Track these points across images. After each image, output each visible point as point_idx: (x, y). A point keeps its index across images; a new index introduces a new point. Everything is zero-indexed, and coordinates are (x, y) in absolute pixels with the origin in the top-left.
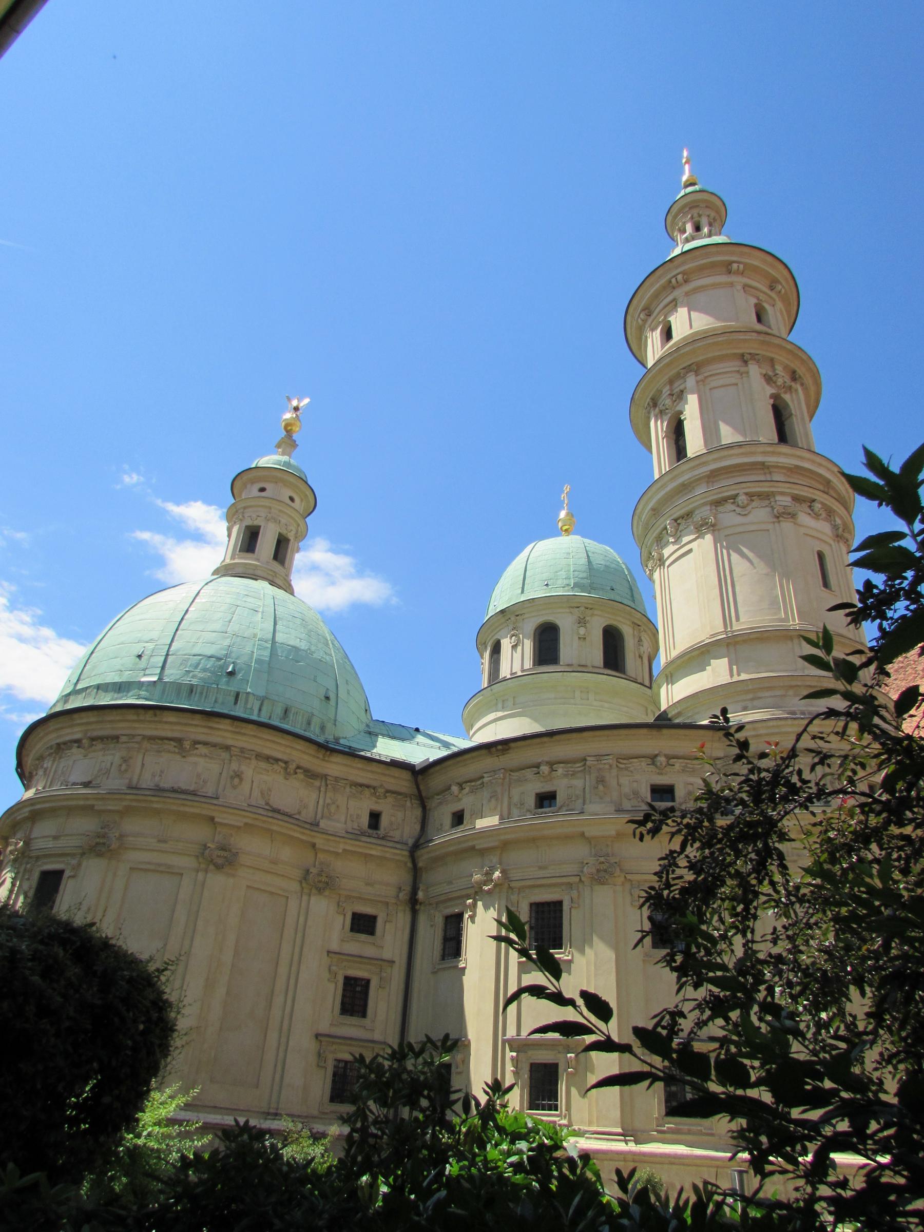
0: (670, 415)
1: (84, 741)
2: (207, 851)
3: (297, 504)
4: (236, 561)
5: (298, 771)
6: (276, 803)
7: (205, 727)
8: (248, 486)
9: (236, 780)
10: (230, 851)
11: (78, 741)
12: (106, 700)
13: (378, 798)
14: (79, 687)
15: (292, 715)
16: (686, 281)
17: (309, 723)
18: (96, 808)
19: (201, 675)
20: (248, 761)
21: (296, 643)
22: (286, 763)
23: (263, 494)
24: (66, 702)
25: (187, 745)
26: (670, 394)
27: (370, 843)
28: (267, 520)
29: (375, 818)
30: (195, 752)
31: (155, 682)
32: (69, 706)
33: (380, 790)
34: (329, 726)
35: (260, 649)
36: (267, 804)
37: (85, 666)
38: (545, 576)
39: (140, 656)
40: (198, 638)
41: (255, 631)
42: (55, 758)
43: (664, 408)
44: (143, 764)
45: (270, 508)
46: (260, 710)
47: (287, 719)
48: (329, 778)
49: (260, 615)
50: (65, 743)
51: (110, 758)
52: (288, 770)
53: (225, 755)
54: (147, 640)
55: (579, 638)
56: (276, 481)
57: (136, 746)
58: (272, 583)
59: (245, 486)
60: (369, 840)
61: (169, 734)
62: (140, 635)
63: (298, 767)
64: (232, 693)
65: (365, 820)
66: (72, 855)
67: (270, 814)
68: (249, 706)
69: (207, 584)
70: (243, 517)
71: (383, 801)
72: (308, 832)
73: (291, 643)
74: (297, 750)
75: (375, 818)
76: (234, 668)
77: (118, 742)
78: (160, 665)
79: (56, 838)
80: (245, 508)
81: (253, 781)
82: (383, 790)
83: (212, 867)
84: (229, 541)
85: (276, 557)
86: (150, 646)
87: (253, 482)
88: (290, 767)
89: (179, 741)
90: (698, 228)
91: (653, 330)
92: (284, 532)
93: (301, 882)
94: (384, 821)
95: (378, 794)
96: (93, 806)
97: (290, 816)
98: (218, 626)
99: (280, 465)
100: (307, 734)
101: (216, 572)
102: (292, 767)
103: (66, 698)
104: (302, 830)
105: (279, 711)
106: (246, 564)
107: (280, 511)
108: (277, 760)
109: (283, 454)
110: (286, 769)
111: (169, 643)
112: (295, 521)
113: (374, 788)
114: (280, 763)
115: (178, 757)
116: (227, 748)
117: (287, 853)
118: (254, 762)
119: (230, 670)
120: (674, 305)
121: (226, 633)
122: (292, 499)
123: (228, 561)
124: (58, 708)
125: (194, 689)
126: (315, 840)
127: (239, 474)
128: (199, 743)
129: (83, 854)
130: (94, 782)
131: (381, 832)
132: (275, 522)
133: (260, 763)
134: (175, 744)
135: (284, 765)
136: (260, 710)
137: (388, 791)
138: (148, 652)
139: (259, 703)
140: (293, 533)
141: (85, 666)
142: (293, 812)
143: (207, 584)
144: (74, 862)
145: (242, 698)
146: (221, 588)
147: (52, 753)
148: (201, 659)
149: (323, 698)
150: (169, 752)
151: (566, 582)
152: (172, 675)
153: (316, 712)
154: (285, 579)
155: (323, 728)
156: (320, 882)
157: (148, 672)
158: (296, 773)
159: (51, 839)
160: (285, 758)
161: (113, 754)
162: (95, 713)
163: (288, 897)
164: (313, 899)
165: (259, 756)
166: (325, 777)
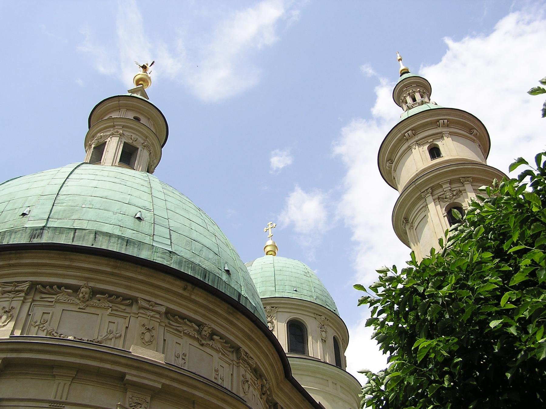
0: (448, 203)
7: (227, 320)
11: (76, 289)
16: (448, 126)
18: (128, 377)
25: (206, 332)
26: (450, 190)
30: (211, 343)
38: (294, 284)
42: (25, 299)
43: (444, 196)
44: (165, 340)
45: (147, 137)
55: (322, 339)
59: (118, 108)
77: (131, 305)
87: (129, 108)
89: (200, 325)
90: (414, 100)
91: (419, 143)
96: (124, 375)
115: (196, 344)
120: (441, 136)
150: (188, 335)
151: (310, 294)
162: (112, 262)
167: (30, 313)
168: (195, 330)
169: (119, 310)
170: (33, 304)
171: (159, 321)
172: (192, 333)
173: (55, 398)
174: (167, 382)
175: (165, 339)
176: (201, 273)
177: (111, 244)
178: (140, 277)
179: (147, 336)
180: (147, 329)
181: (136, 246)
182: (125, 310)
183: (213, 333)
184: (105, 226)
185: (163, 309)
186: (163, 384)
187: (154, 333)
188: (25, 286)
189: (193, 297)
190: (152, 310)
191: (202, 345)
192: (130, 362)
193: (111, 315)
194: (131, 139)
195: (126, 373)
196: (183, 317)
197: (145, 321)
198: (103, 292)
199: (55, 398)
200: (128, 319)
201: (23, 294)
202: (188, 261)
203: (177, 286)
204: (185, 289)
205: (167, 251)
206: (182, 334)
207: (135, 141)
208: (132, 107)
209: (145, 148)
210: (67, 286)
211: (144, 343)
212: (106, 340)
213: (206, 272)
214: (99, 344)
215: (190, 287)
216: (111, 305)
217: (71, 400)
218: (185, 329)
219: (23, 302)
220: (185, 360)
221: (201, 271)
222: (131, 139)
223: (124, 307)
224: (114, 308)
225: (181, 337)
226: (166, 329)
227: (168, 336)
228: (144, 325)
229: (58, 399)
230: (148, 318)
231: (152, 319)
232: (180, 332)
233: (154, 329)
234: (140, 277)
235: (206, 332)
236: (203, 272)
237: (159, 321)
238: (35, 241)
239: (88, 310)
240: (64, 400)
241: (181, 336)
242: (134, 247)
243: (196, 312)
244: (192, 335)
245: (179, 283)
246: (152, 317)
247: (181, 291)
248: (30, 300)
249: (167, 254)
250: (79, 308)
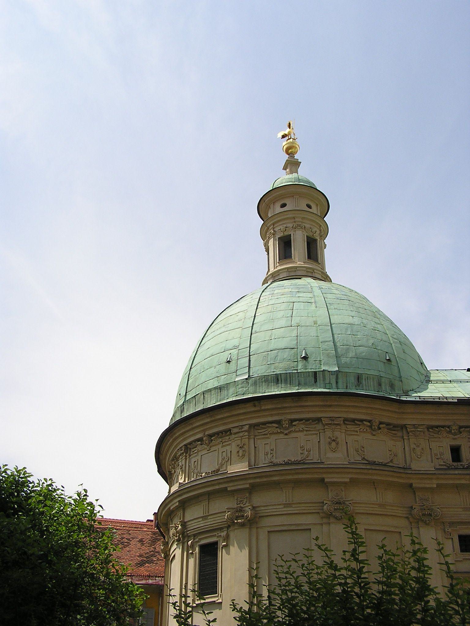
2: (325, 507)
3: (314, 210)
4: (279, 268)
5: (381, 426)
6: (371, 457)
8: (272, 206)
9: (334, 444)
10: (344, 503)
12: (212, 402)
13: (455, 434)
14: (188, 397)
15: (364, 380)
17: (380, 385)
18: (229, 489)
19: (281, 365)
20: (339, 427)
21: (349, 320)
22: (370, 421)
23: (285, 209)
24: (182, 411)
25: (286, 425)
27: (459, 474)
28: (294, 228)
29: (456, 452)
30: (293, 429)
31: (246, 379)
32: (185, 414)
33: (454, 428)
34: (397, 383)
35: (323, 333)
36: (364, 459)
37: (188, 380)
39: (229, 362)
40: (271, 336)
41: (314, 319)
42: (186, 456)
44: (255, 447)
45: (294, 218)
46: (337, 383)
47: (361, 385)
48: (407, 426)
49: (314, 305)
50: (190, 443)
51: (228, 448)
52: (373, 427)
53: (319, 426)
54: (231, 347)
56: (292, 196)
57: (246, 434)
58: (315, 278)
59: (268, 207)
60: (456, 472)
61: (270, 419)
62: (224, 345)
63: (381, 423)
64: (311, 374)
65: (448, 456)
66: (221, 529)
67: (368, 467)
68: (327, 381)
69: (263, 292)
70: (274, 231)
71: (459, 436)
72: (403, 475)
73: (347, 321)
74: (376, 409)
75: (456, 452)
76: (306, 353)
77: (231, 434)
78: (247, 365)
79: (204, 518)
80: (273, 224)
81: (347, 443)
82: (457, 427)
83: (332, 520)
84: (268, 254)
85: (309, 257)
86: (234, 352)
88: (374, 424)
89: (279, 422)
92: (310, 234)
93: (407, 518)
94: (465, 453)
95: (453, 431)
97: (385, 465)
98: (283, 323)
99: (292, 182)
100: (381, 394)
101: (265, 282)
102: (375, 424)
103: (181, 408)
104: (398, 475)
105: (352, 380)
106: (288, 268)
107: (303, 218)
108: (362, 421)
109: (291, 172)
110: (371, 427)
111: (249, 346)
112: (317, 223)
113: (449, 427)
114: (365, 423)
115: (282, 436)
116: (319, 420)
117: (390, 497)
118: (344, 427)
119: (303, 355)
121: (291, 326)
122: (309, 206)
123: (272, 270)
124: (178, 418)
126: (411, 481)
127: (261, 198)
128: (295, 420)
129: (229, 527)
130: (221, 470)
131: (465, 463)
132: (302, 228)
133: (348, 426)
134: (277, 425)
135: (368, 424)
136: (337, 383)
137: (461, 427)
138: (234, 358)
139: (335, 376)
140: (318, 232)
141: (188, 380)
142: (386, 462)
143: (263, 292)
144: (224, 534)
145: (320, 377)
146: (276, 292)
147: (183, 453)
148: (278, 352)
149: (385, 361)
150: (273, 433)
152: (258, 370)
153: (382, 374)
154: (322, 273)
155: (392, 386)
156: (424, 515)
157: (238, 373)
158: (380, 428)
159: (201, 519)
160: (368, 418)
161: (229, 444)
163: (400, 532)
164: (421, 529)
165: (346, 421)
166: (403, 427)
172: (275, 430)
173: (204, 514)
174: (251, 481)
176: (274, 380)
177: (212, 396)
178: (226, 415)
181: (225, 388)
183: (292, 421)
184: (209, 383)
186: (250, 484)
189: (263, 408)
191: (286, 434)
193: (222, 447)
194: (282, 231)
196: (264, 424)
199: (204, 514)
203: (250, 408)
204: (255, 406)
205: (244, 380)
207: (286, 230)
209: (296, 229)
213: (278, 376)
215: (256, 403)
217: (211, 513)
218: (269, 430)
219: (186, 459)
222: (282, 231)
223: (227, 438)
224: (223, 441)
225: (268, 438)
228: (238, 446)
229: (205, 515)
232: (267, 434)
234: (226, 415)
235: (286, 425)
236: (275, 378)
242: (224, 389)
243: (272, 415)
245: (248, 405)
247: (253, 409)
249: (245, 382)
250: (208, 451)
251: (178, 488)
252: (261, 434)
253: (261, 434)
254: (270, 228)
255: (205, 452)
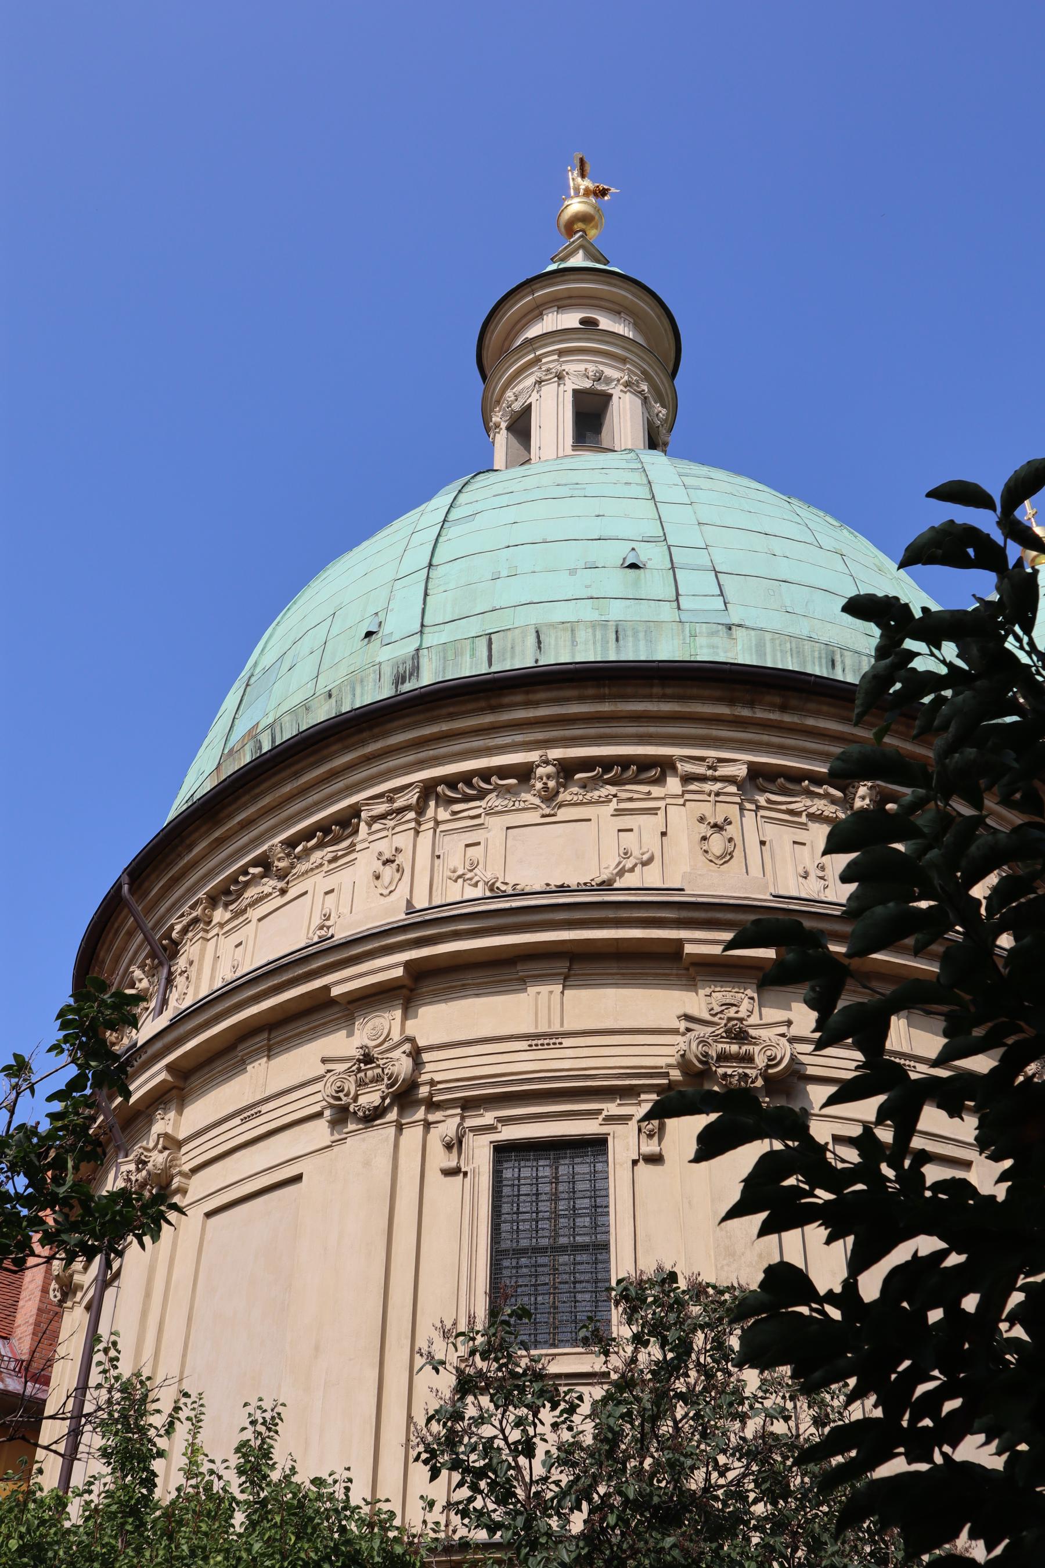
1: (540, 771)
11: (524, 774)
37: (426, 594)
56: (617, 310)
77: (660, 781)
80: (561, 353)
87: (562, 303)
125: (838, 658)
159: (523, 1045)
167: (437, 853)
168: (834, 801)
169: (636, 796)
170: (438, 830)
171: (737, 800)
175: (763, 839)
176: (820, 658)
179: (717, 844)
180: (712, 827)
182: (649, 793)
185: (741, 771)
187: (731, 830)
188: (412, 797)
190: (715, 779)
192: (685, 914)
193: (619, 813)
195: (681, 940)
197: (706, 809)
198: (586, 764)
200: (661, 813)
201: (412, 815)
202: (779, 638)
206: (803, 819)
208: (570, 297)
210: (503, 772)
211: (711, 861)
212: (621, 873)
213: (833, 652)
214: (606, 886)
216: (613, 790)
219: (417, 833)
220: (825, 880)
221: (820, 653)
222: (588, 378)
223: (645, 788)
225: (803, 826)
226: (762, 817)
227: (771, 831)
228: (702, 819)
229: (543, 1028)
230: (709, 799)
231: (717, 799)
232: (798, 814)
233: (730, 823)
236: (824, 655)
237: (737, 800)
238: (407, 687)
239: (564, 814)
240: (556, 1028)
241: (805, 824)
244: (831, 815)
246: (718, 794)
248: (431, 824)
250: (543, 816)
251: (404, 916)
252: (784, 807)
253: (784, 807)
254: (544, 360)
255: (534, 817)
